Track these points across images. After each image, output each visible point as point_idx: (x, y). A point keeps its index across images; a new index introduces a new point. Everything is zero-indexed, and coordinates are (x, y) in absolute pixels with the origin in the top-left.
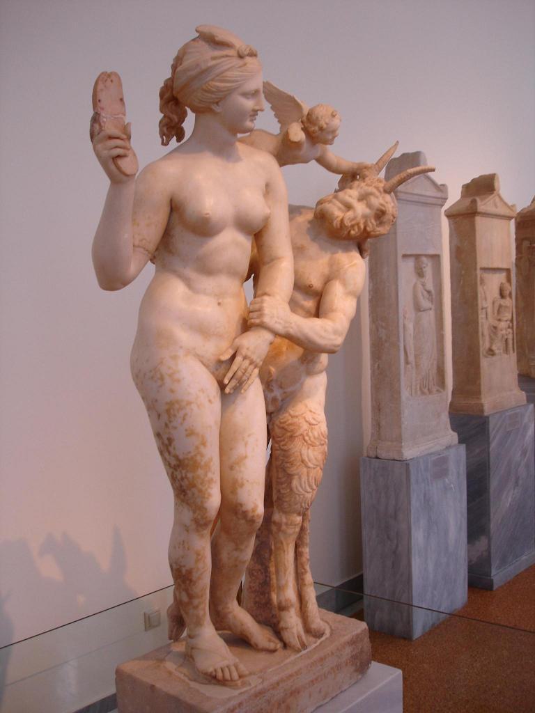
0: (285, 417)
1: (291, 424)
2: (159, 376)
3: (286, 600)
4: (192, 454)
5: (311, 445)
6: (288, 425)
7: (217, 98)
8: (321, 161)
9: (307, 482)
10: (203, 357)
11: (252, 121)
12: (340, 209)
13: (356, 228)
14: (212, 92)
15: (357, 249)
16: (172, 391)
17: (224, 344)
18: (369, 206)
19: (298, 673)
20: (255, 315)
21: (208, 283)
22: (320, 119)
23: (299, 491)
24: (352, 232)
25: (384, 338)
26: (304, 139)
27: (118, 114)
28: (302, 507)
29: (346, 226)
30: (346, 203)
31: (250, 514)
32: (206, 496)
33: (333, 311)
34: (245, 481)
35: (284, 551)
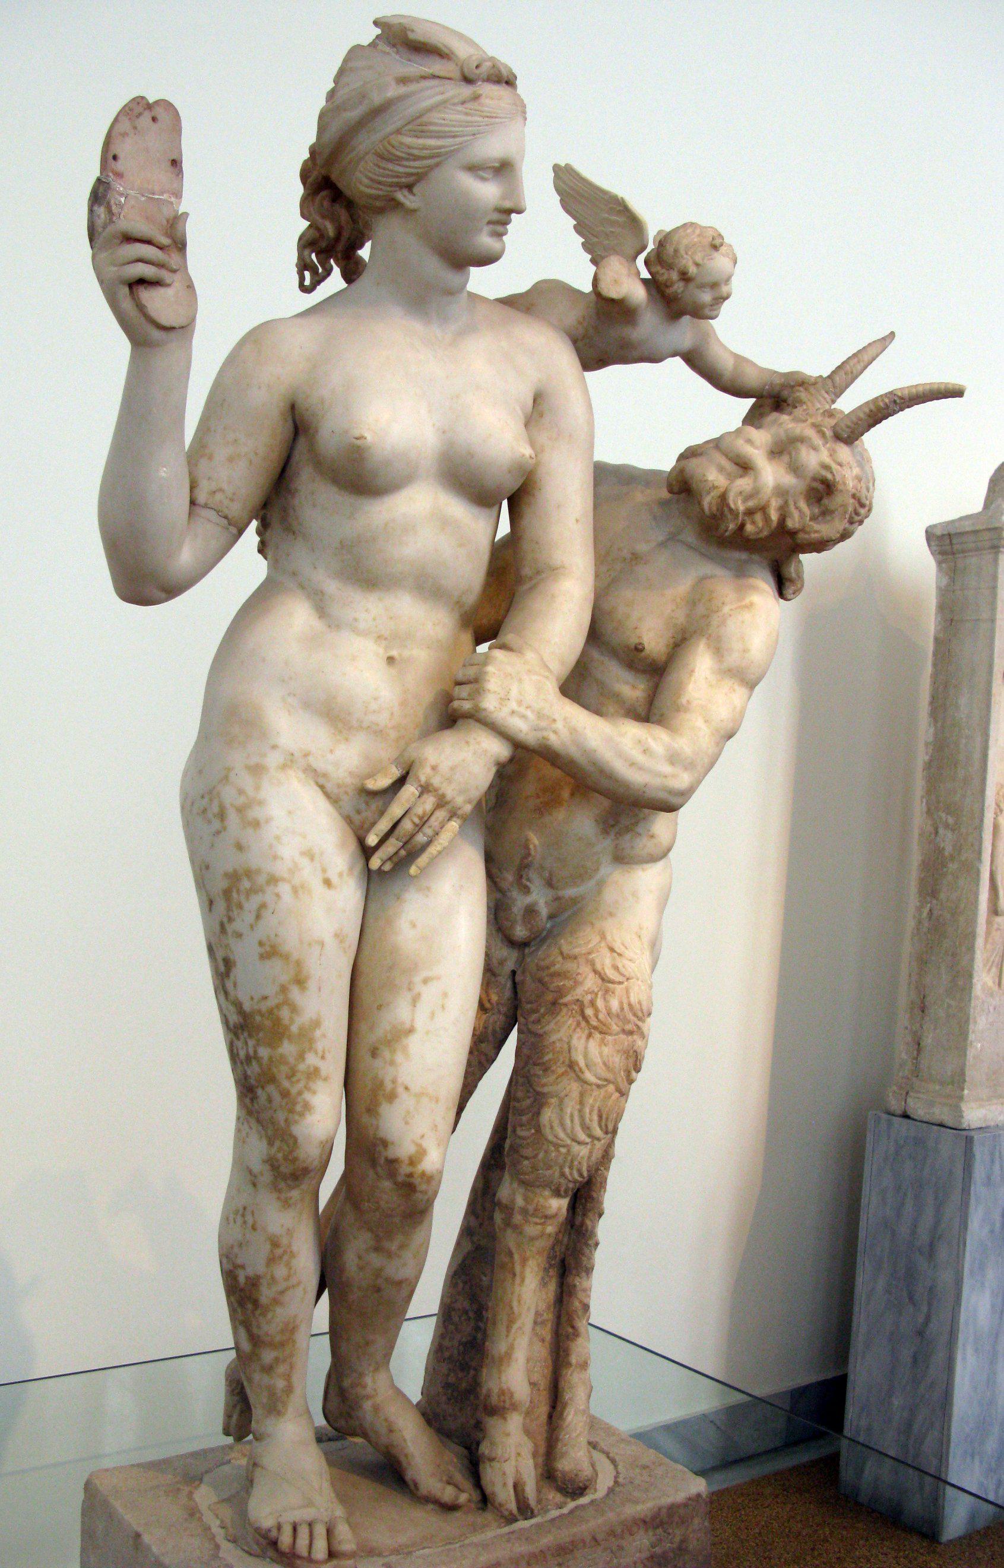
0: (549, 955)
1: (557, 974)
2: (216, 809)
3: (502, 1392)
4: (271, 1003)
5: (595, 1028)
6: (552, 975)
7: (412, 174)
8: (695, 360)
9: (576, 1113)
10: (325, 775)
11: (500, 235)
12: (721, 469)
13: (758, 517)
14: (397, 160)
15: (771, 580)
16: (240, 847)
17: (385, 752)
18: (795, 469)
20: (464, 691)
21: (369, 609)
22: (682, 252)
23: (556, 1137)
24: (749, 528)
25: (948, 850)
26: (648, 300)
27: (162, 194)
28: (563, 1174)
29: (731, 510)
30: (738, 456)
31: (405, 1169)
32: (298, 1108)
33: (678, 710)
34: (400, 1090)
35: (514, 1275)
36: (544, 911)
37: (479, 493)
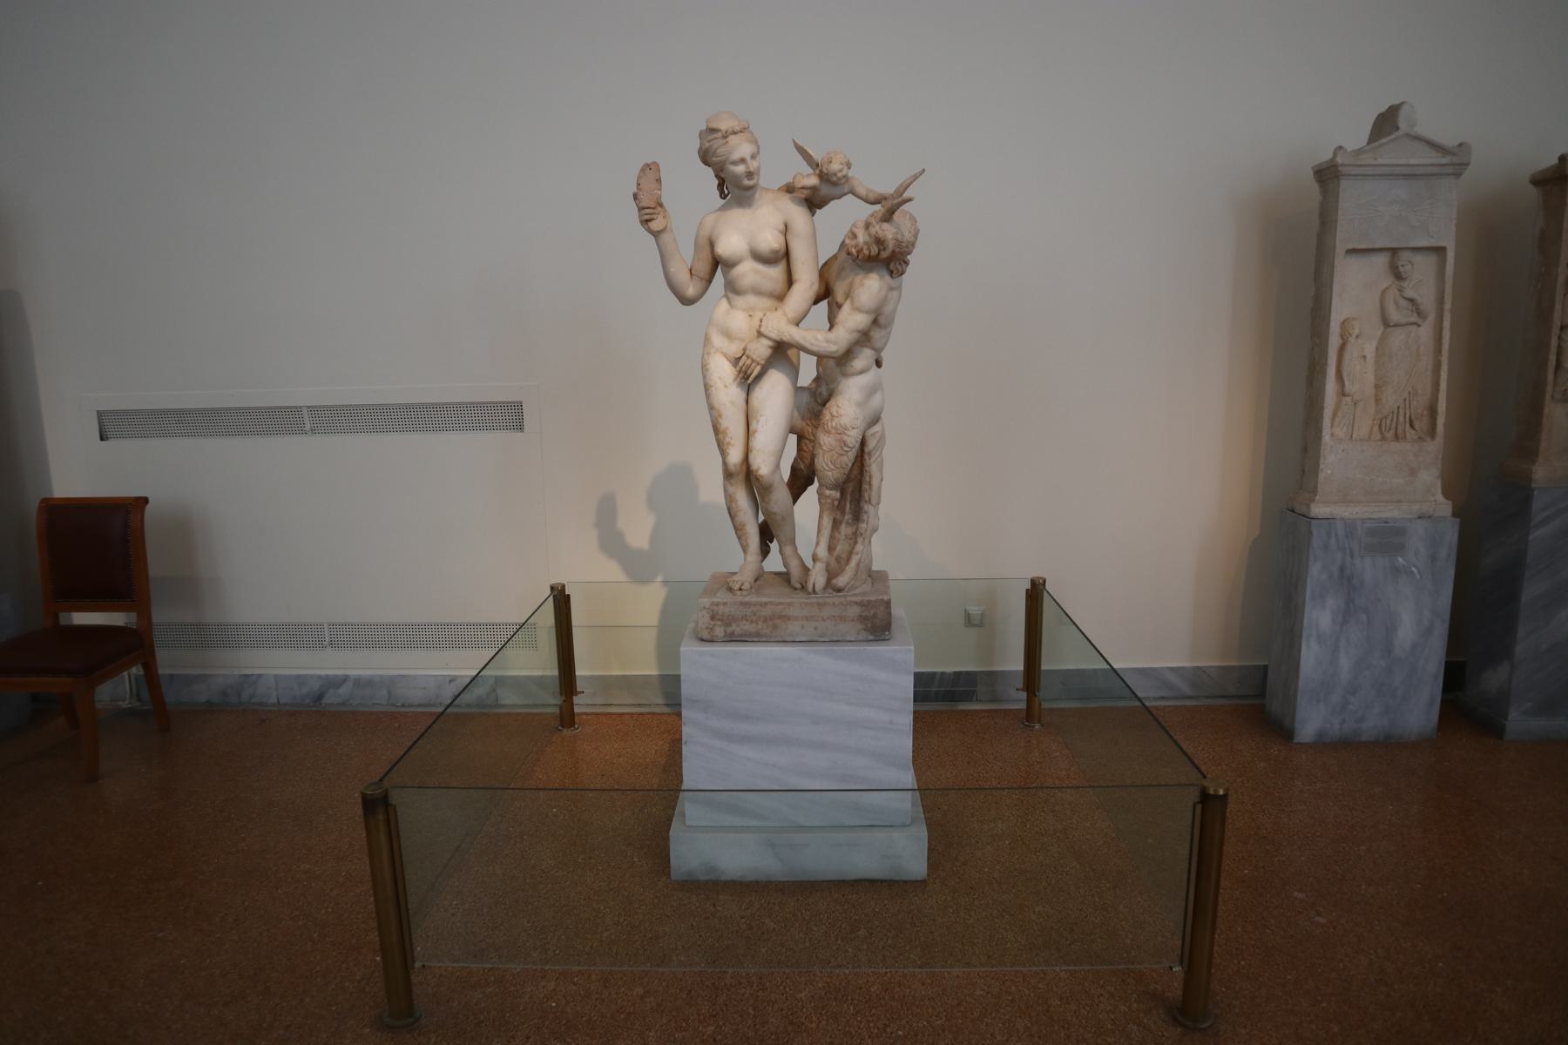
19: (790, 604)
36: (825, 394)
37: (766, 259)
